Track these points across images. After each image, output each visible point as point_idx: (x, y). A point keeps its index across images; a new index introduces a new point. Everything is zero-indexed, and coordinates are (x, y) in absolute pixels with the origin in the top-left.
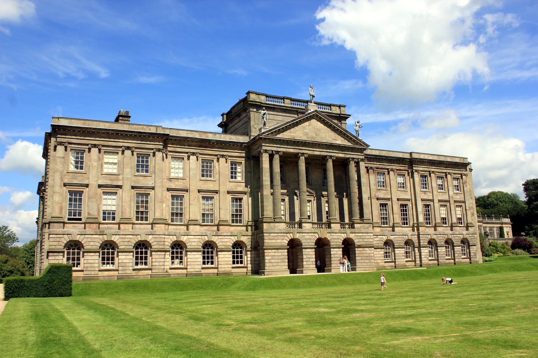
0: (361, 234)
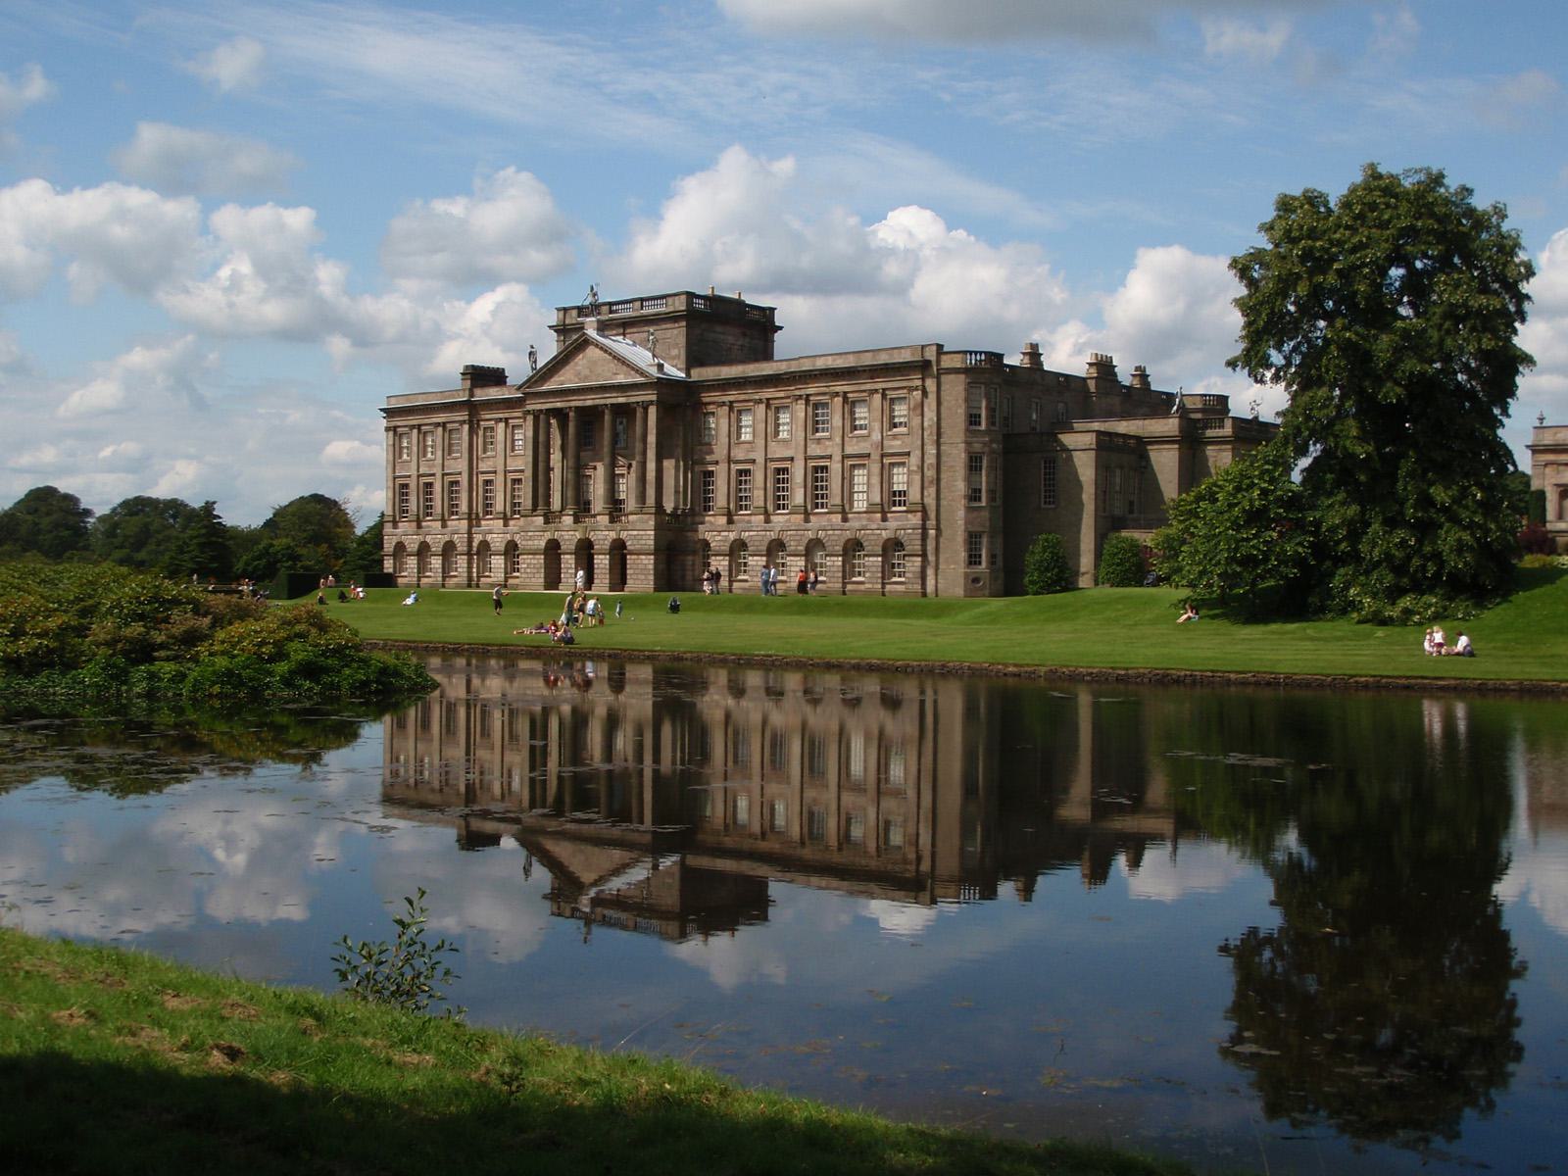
0: (635, 533)
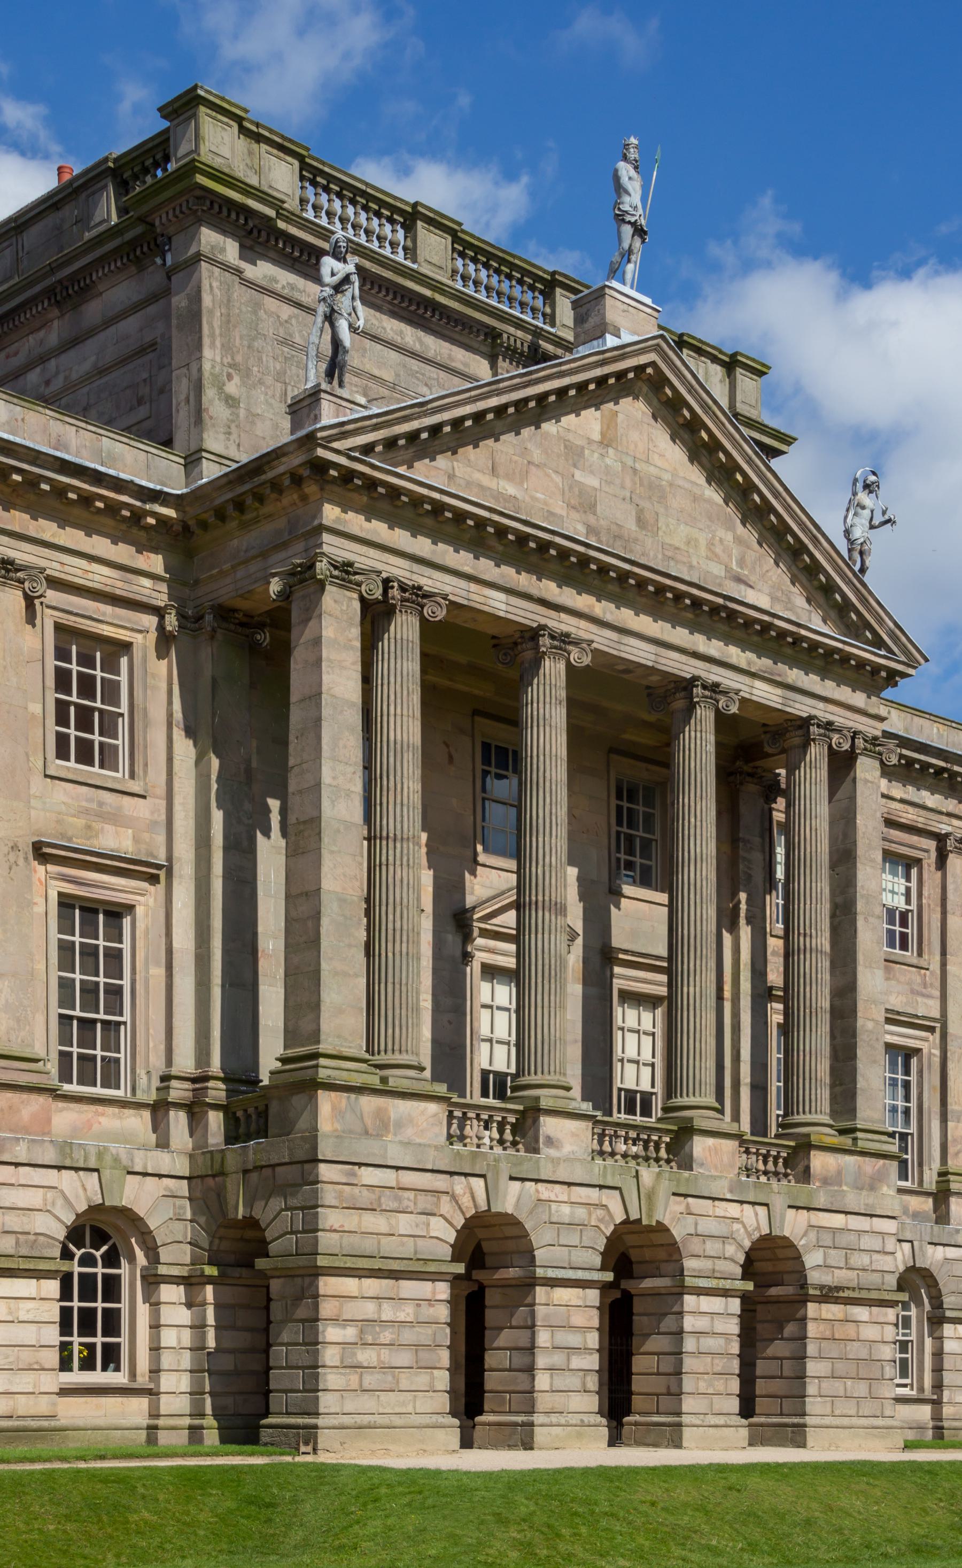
0: (837, 1220)
